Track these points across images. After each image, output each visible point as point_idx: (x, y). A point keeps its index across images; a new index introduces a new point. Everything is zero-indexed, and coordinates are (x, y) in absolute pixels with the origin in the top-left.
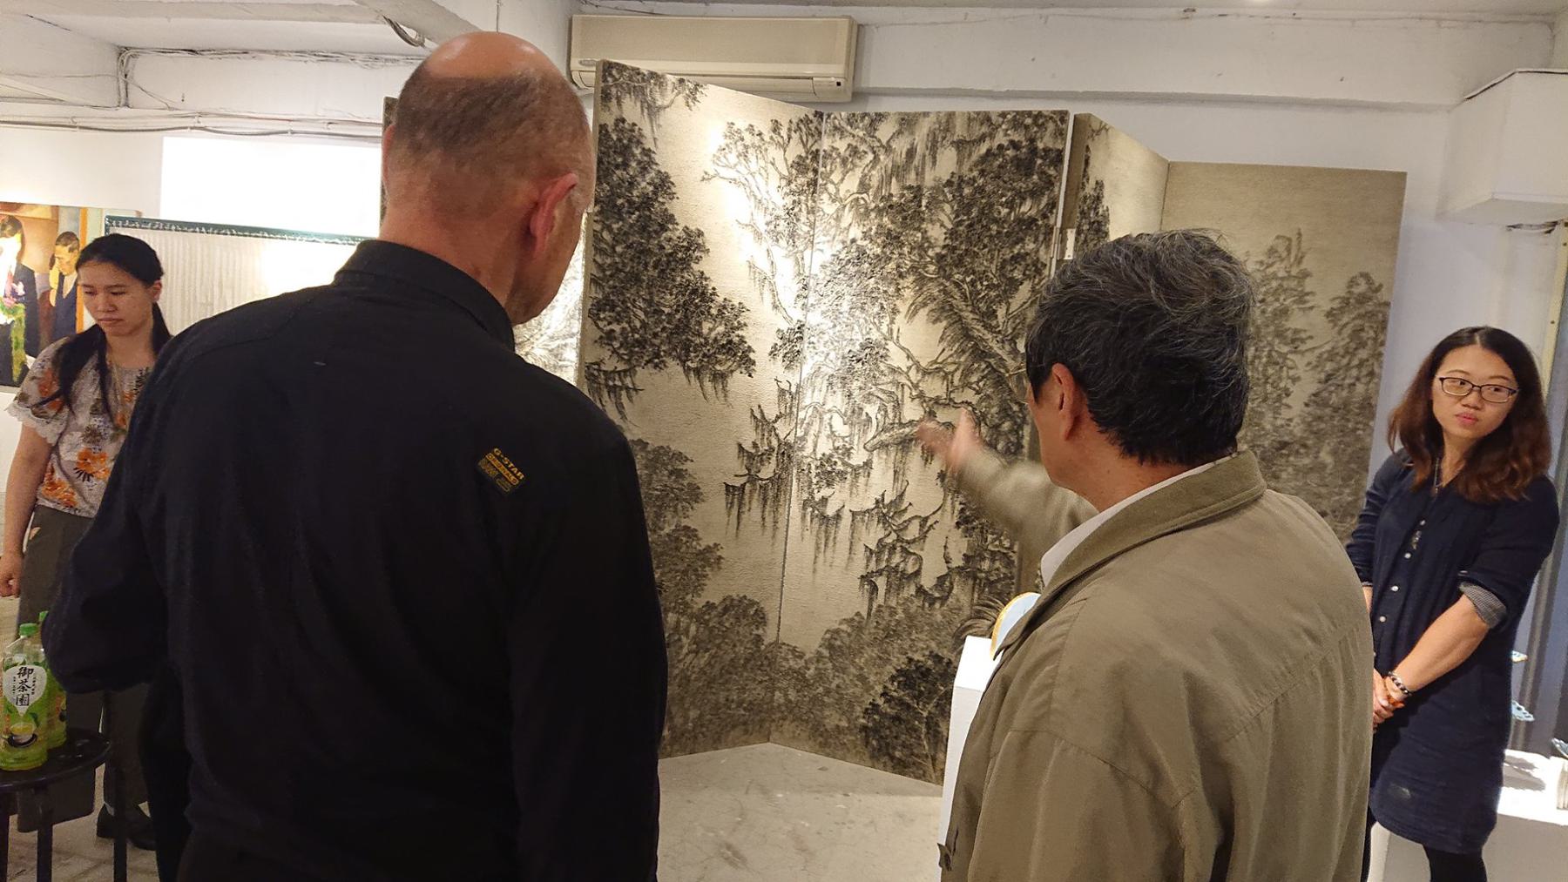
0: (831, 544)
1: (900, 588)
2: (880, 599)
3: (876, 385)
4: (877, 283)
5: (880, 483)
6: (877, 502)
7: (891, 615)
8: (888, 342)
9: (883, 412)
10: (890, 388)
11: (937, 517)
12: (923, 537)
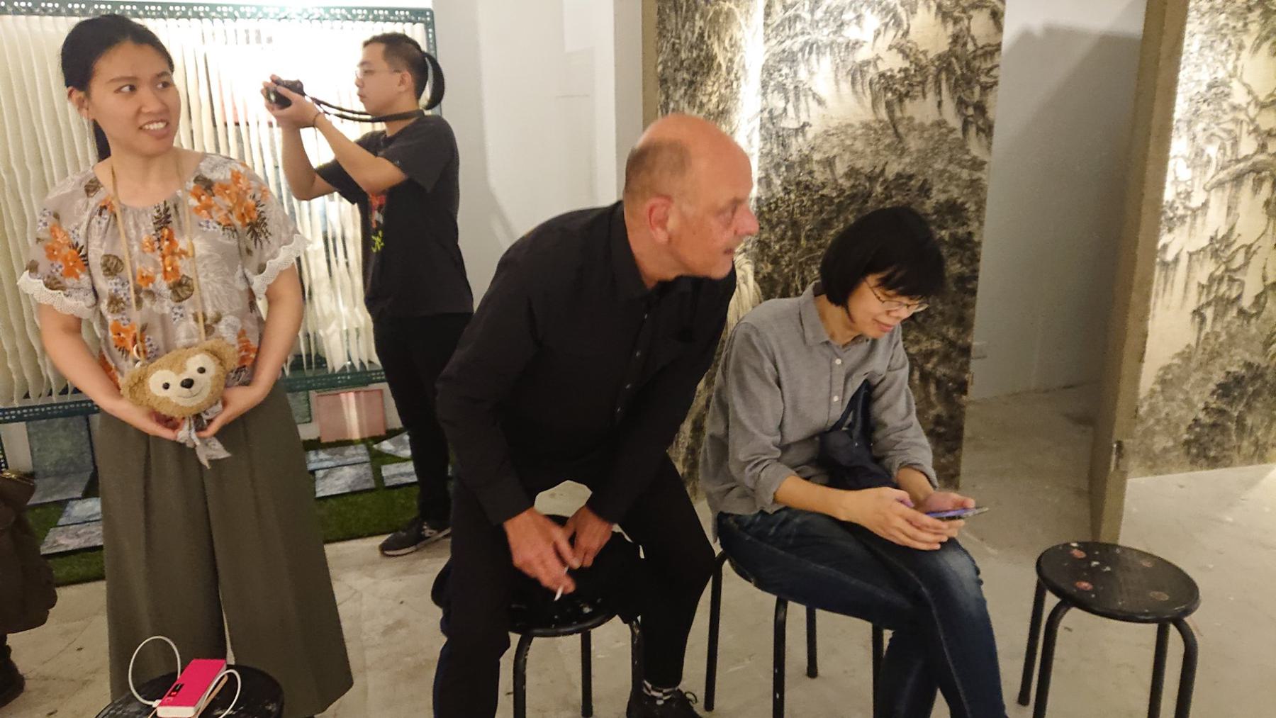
0: (1169, 286)
1: (1224, 313)
2: (1208, 328)
3: (1218, 124)
4: (1227, 18)
5: (1215, 222)
6: (1212, 239)
7: (1216, 339)
8: (1233, 79)
9: (1222, 151)
10: (1231, 126)
11: (1260, 243)
12: (1246, 263)
